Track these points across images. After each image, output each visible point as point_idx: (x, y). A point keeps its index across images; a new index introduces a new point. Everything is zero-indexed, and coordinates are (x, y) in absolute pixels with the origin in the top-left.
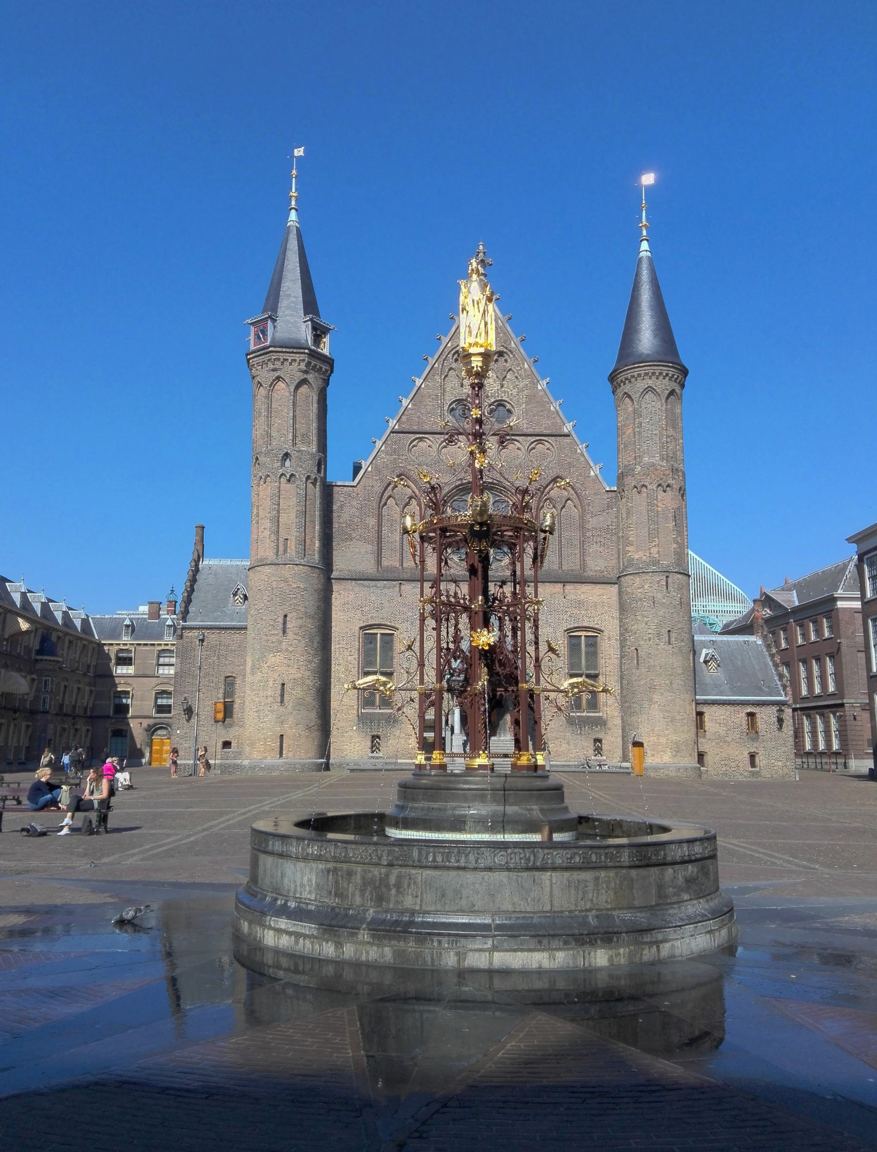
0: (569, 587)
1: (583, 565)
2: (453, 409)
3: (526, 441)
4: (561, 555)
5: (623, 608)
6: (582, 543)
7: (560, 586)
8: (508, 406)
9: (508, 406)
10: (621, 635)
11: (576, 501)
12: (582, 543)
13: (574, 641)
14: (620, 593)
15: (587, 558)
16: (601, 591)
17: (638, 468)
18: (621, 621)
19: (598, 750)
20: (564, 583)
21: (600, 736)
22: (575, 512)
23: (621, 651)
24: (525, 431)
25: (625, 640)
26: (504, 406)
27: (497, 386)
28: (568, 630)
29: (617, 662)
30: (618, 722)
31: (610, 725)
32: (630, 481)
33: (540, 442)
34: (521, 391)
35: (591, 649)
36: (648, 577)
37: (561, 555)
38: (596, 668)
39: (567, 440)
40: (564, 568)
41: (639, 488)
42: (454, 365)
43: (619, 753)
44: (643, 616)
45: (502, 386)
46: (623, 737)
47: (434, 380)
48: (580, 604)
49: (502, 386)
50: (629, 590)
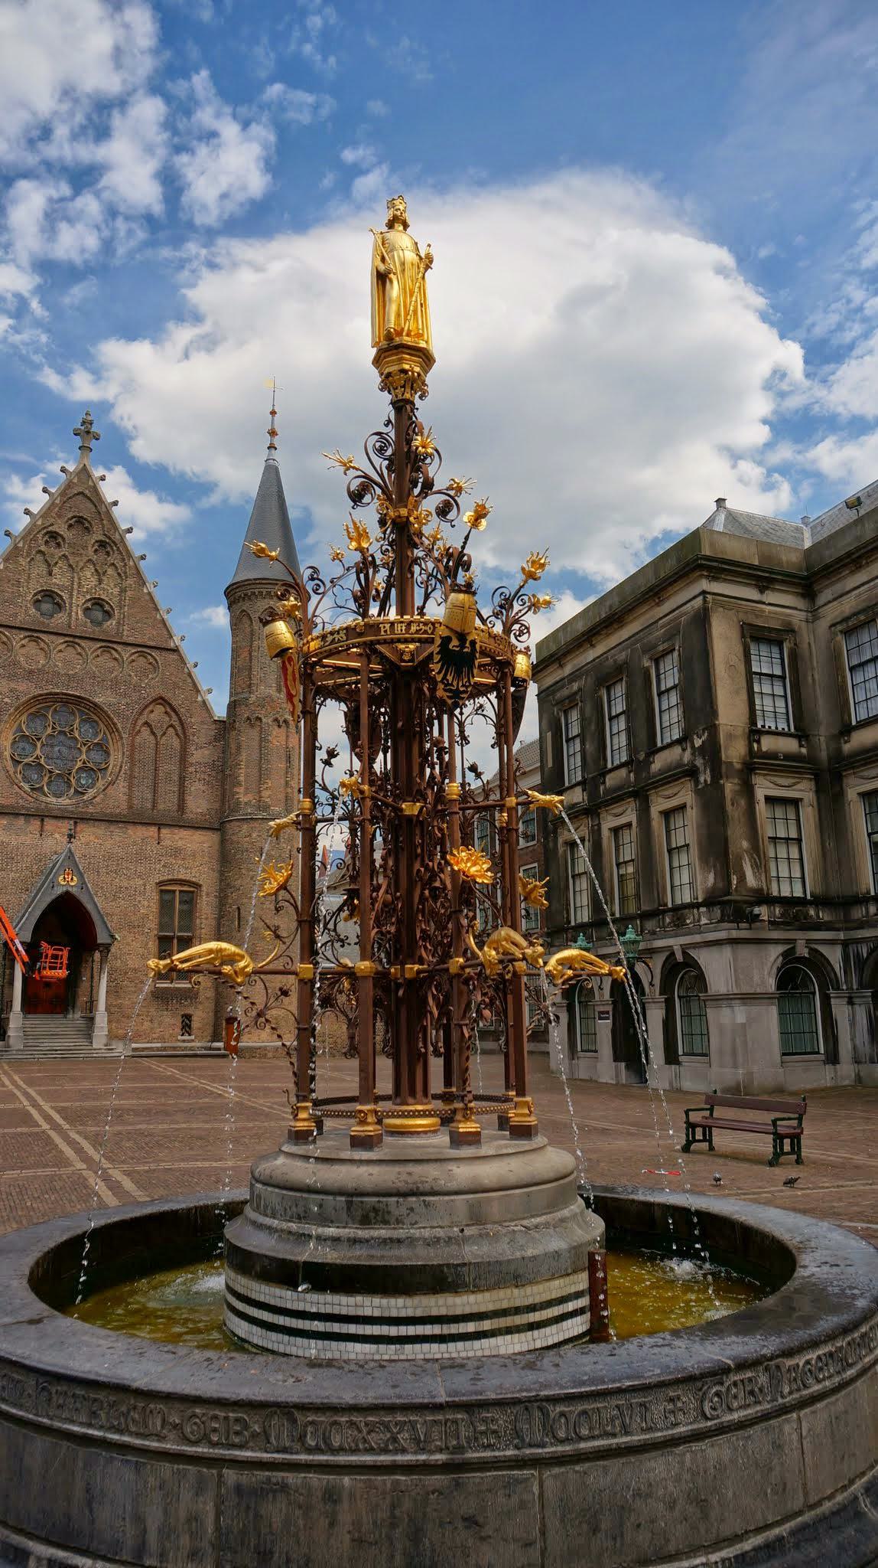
0: (164, 831)
1: (181, 806)
2: (38, 601)
3: (126, 653)
4: (155, 792)
5: (226, 859)
6: (182, 779)
7: (153, 830)
8: (107, 608)
9: (107, 608)
10: (221, 890)
11: (180, 732)
12: (182, 779)
13: (167, 897)
14: (223, 842)
15: (187, 798)
16: (203, 838)
17: (253, 698)
18: (222, 873)
19: (186, 1026)
20: (160, 826)
21: (189, 1011)
22: (176, 743)
23: (221, 910)
24: (125, 639)
25: (226, 897)
26: (102, 606)
27: (94, 581)
28: (160, 883)
29: (214, 923)
30: (211, 994)
31: (201, 998)
32: (244, 712)
33: (142, 654)
34: (123, 591)
35: (185, 907)
36: (256, 824)
37: (155, 792)
38: (189, 928)
39: (175, 656)
40: (161, 807)
41: (254, 721)
42: (43, 548)
43: (210, 1030)
44: (249, 870)
45: (100, 581)
46: (216, 1012)
47: (17, 562)
48: (177, 852)
49: (100, 581)
50: (234, 838)
